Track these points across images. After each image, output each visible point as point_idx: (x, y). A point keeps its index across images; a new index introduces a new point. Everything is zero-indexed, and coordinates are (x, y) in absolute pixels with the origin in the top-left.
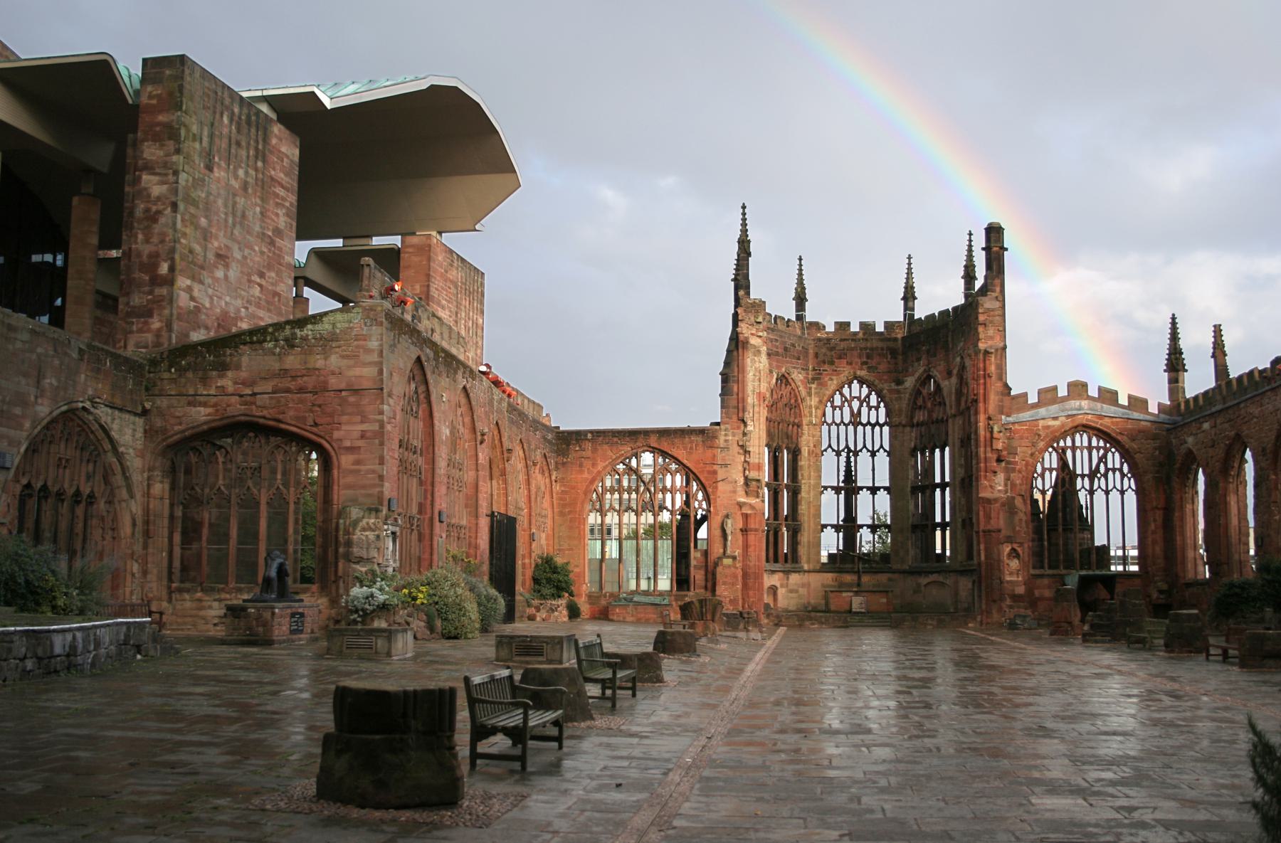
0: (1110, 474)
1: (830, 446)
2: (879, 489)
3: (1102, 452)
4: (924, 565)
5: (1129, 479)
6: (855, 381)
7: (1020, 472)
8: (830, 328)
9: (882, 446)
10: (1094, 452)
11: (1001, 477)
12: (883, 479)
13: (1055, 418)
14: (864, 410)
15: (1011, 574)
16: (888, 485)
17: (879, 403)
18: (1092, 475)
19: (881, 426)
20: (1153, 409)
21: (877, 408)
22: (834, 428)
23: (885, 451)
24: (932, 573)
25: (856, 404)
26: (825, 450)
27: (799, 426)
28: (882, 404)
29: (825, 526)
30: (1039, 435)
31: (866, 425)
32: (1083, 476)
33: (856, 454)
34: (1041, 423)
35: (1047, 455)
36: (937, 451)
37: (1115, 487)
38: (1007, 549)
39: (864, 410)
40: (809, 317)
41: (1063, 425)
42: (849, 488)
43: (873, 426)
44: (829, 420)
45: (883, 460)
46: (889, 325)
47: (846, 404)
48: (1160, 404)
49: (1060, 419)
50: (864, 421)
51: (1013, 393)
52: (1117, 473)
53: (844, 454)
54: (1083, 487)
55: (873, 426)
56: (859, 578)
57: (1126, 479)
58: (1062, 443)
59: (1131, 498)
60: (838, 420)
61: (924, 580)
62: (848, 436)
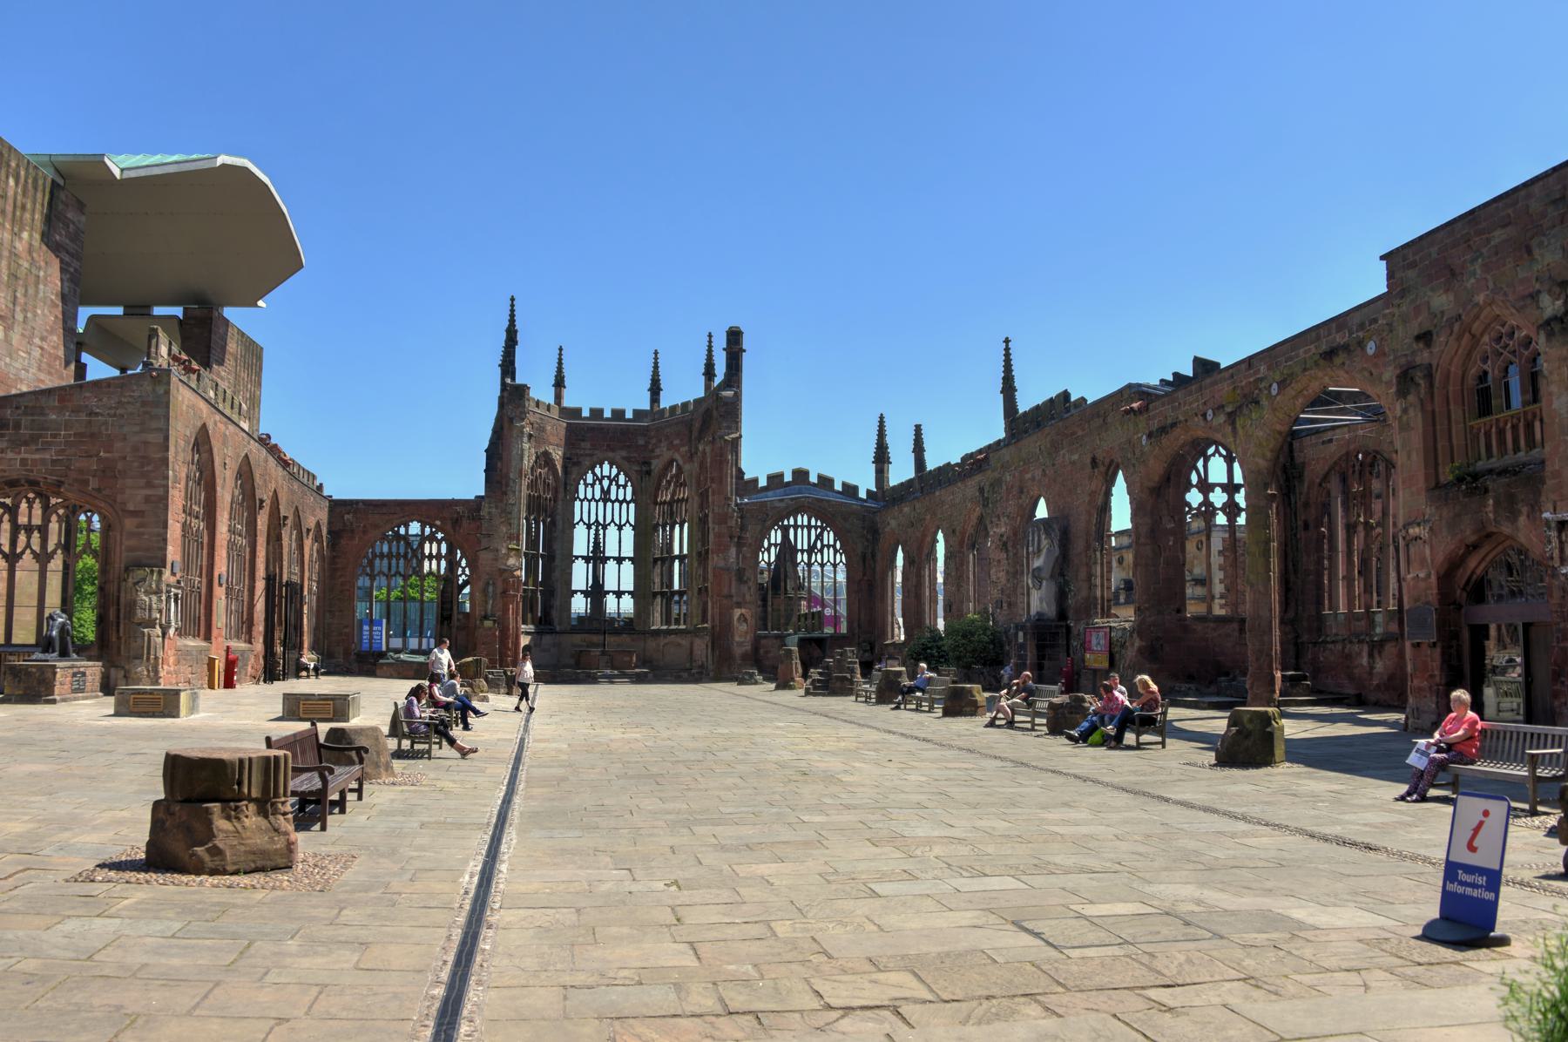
0: (826, 550)
1: (581, 520)
2: (624, 559)
3: (819, 530)
5: (841, 555)
7: (750, 544)
9: (628, 521)
10: (813, 531)
12: (628, 550)
14: (614, 488)
16: (632, 555)
17: (626, 482)
18: (811, 550)
19: (628, 503)
20: (863, 494)
21: (625, 487)
22: (586, 504)
23: (631, 525)
25: (606, 483)
26: (578, 523)
28: (629, 484)
29: (576, 592)
32: (802, 551)
33: (605, 527)
35: (773, 532)
36: (677, 526)
37: (829, 561)
39: (614, 488)
41: (787, 507)
42: (597, 557)
43: (621, 503)
44: (582, 496)
45: (628, 533)
46: (636, 412)
48: (869, 492)
50: (613, 497)
52: (831, 549)
53: (594, 527)
54: (802, 560)
55: (621, 503)
57: (838, 555)
58: (786, 523)
60: (589, 497)
62: (598, 511)
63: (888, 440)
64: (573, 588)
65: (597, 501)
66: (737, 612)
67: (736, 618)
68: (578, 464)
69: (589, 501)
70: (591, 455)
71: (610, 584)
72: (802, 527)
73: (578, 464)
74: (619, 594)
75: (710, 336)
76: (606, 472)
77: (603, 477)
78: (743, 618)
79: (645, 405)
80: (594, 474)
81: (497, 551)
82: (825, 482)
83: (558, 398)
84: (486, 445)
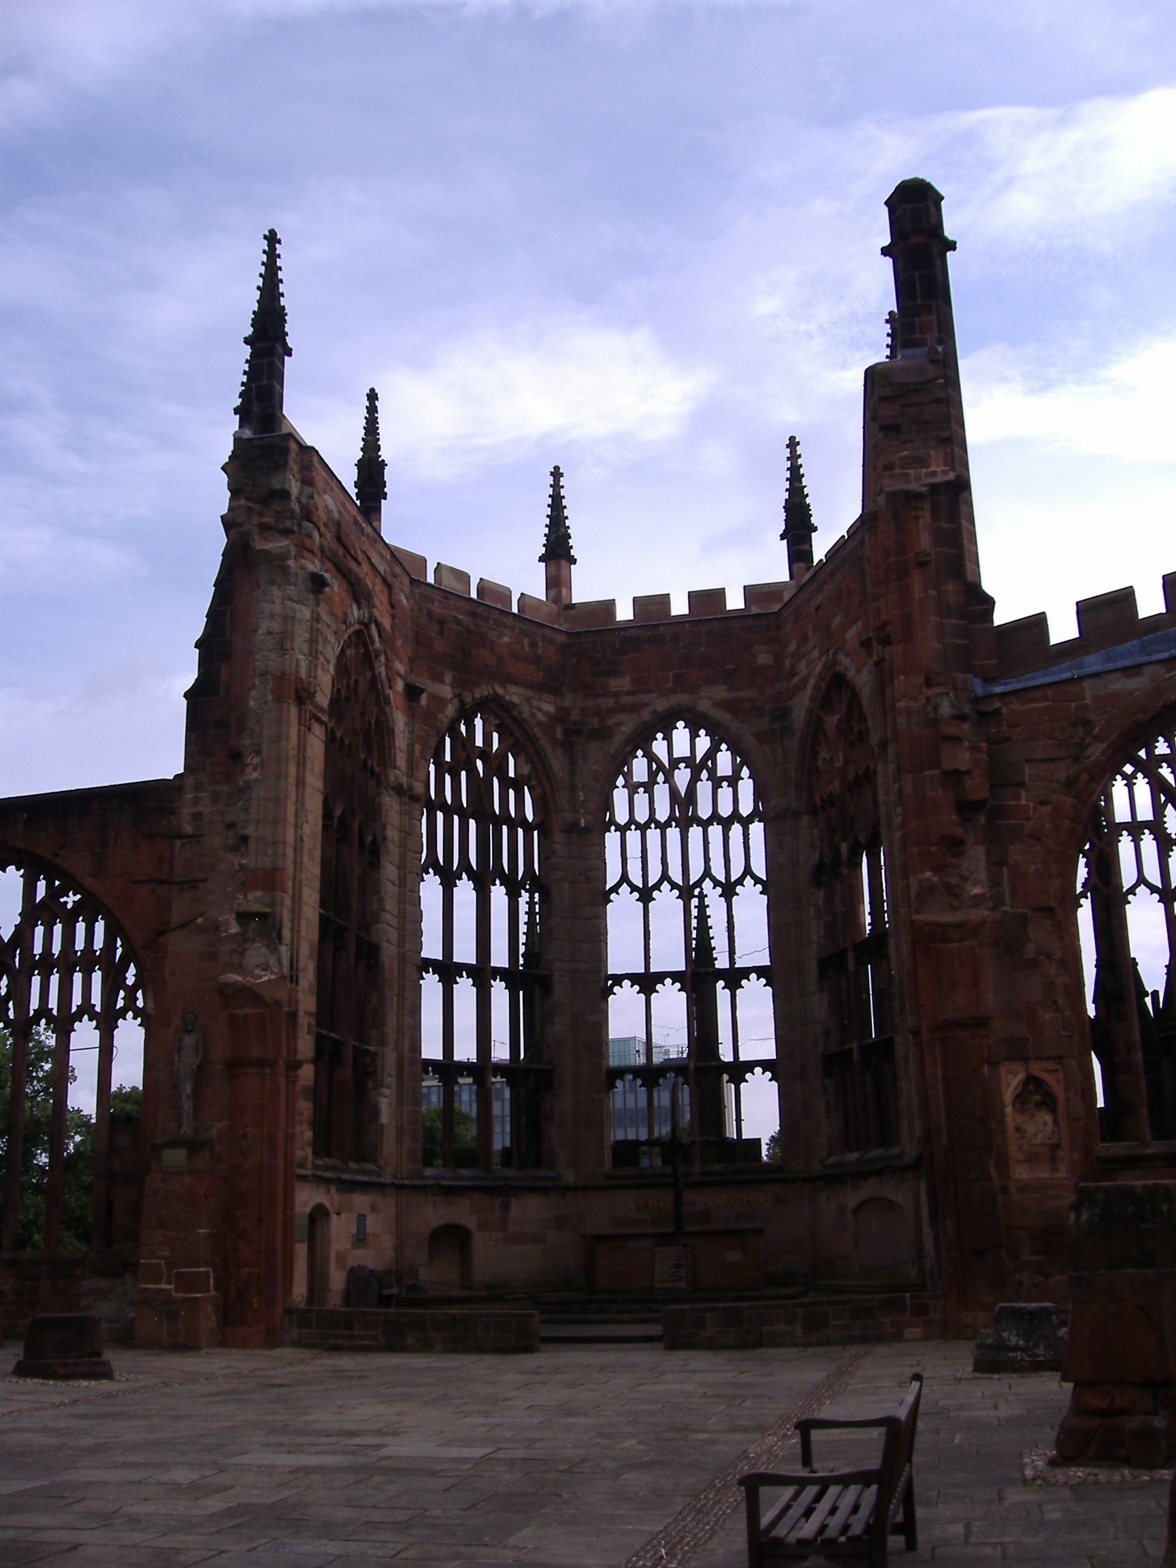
1: (624, 878)
4: (853, 1156)
6: (681, 724)
7: (1036, 837)
9: (748, 871)
11: (976, 859)
13: (1132, 671)
15: (1031, 1159)
16: (765, 961)
21: (733, 781)
22: (633, 836)
23: (757, 880)
24: (867, 1175)
25: (682, 777)
26: (615, 889)
28: (745, 772)
30: (1087, 724)
34: (1089, 690)
35: (1119, 790)
38: (1011, 1081)
39: (704, 788)
43: (726, 824)
44: (622, 817)
47: (661, 777)
49: (1147, 670)
50: (704, 812)
51: (1000, 617)
55: (726, 824)
60: (642, 816)
61: (852, 1198)
65: (663, 827)
67: (1008, 1095)
68: (603, 733)
69: (643, 828)
73: (603, 733)
80: (651, 757)
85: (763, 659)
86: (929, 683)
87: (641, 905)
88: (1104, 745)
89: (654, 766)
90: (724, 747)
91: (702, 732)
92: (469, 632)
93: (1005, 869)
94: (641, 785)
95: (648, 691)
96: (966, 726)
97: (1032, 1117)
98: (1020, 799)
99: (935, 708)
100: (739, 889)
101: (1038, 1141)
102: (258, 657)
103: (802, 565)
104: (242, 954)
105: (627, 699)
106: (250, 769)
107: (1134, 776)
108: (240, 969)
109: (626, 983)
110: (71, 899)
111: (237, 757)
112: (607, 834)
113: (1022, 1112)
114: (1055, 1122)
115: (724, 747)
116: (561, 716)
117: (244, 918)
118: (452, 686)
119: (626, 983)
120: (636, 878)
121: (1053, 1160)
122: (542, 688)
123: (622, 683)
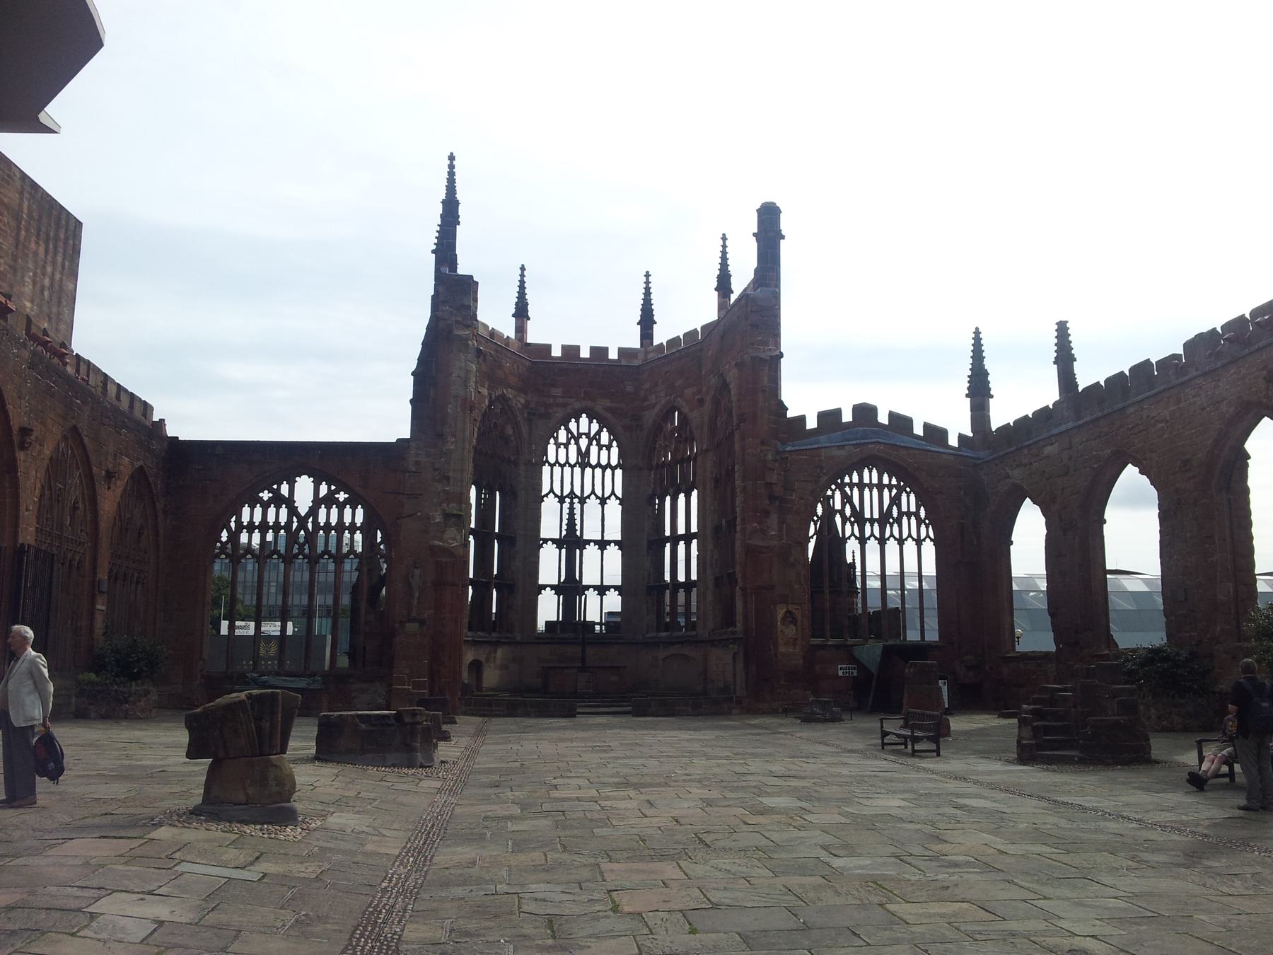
0: (905, 520)
1: (552, 490)
2: (609, 543)
3: (894, 491)
6: (584, 415)
8: (556, 352)
9: (613, 493)
10: (886, 492)
11: (773, 520)
12: (614, 532)
14: (594, 449)
16: (619, 538)
17: (611, 442)
18: (884, 519)
19: (613, 469)
20: (953, 441)
22: (557, 469)
23: (617, 498)
24: (673, 644)
25: (584, 442)
26: (546, 495)
27: (516, 463)
28: (615, 444)
29: (544, 587)
31: (595, 467)
32: (872, 521)
33: (582, 501)
37: (910, 535)
38: (781, 612)
39: (594, 449)
40: (533, 337)
42: (572, 542)
43: (604, 468)
44: (552, 459)
45: (614, 510)
46: (622, 351)
48: (961, 438)
50: (593, 461)
52: (913, 520)
54: (872, 535)
55: (604, 468)
56: (583, 651)
57: (923, 527)
58: (847, 480)
59: (929, 549)
60: (562, 460)
62: (572, 480)
63: (988, 364)
64: (541, 582)
65: (572, 467)
66: (781, 612)
67: (779, 618)
69: (562, 466)
70: (564, 405)
71: (590, 577)
72: (871, 486)
74: (602, 590)
75: (724, 238)
76: (584, 429)
77: (580, 435)
78: (790, 618)
79: (634, 342)
80: (568, 431)
81: (428, 518)
82: (900, 423)
83: (521, 330)
84: (413, 365)
85: (629, 389)
86: (763, 443)
87: (559, 504)
88: (827, 477)
89: (570, 436)
90: (605, 429)
91: (595, 421)
92: (495, 361)
93: (784, 525)
94: (563, 444)
95: (571, 397)
96: (777, 464)
97: (787, 626)
98: (792, 496)
99: (765, 456)
100: (608, 501)
101: (789, 637)
102: (452, 388)
103: (648, 341)
104: (443, 532)
105: (561, 400)
106: (450, 444)
107: (835, 490)
108: (441, 539)
109: (550, 543)
110: (342, 496)
111: (441, 436)
112: (544, 467)
113: (783, 624)
114: (796, 630)
115: (605, 429)
116: (526, 406)
117: (447, 516)
118: (488, 389)
119: (550, 543)
120: (558, 492)
121: (794, 645)
122: (522, 390)
123: (558, 391)
